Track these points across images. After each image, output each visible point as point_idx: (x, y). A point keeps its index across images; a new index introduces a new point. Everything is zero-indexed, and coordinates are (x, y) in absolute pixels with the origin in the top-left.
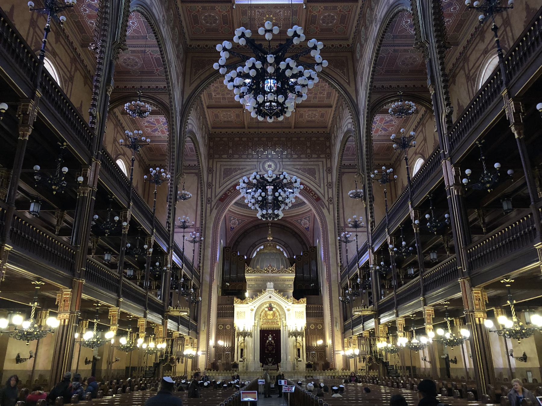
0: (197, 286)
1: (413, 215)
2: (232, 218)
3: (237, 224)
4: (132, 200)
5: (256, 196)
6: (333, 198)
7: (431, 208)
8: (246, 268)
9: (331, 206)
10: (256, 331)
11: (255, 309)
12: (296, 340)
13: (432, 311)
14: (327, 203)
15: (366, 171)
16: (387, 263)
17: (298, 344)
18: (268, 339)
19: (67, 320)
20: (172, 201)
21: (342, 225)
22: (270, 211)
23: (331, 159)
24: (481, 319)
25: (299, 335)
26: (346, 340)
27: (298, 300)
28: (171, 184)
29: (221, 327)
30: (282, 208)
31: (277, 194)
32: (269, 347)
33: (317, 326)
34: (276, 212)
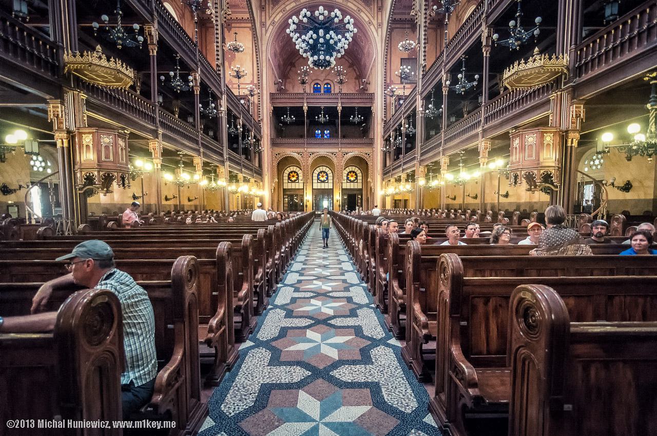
0: (258, 137)
1: (486, 35)
4: (155, 13)
5: (307, 38)
7: (518, 14)
13: (490, 144)
15: (423, 7)
16: (438, 105)
19: (65, 141)
20: (219, 40)
21: (388, 81)
22: (322, 57)
23: (381, 12)
24: (574, 140)
26: (384, 183)
28: (216, 21)
30: (334, 57)
31: (328, 36)
34: (328, 58)
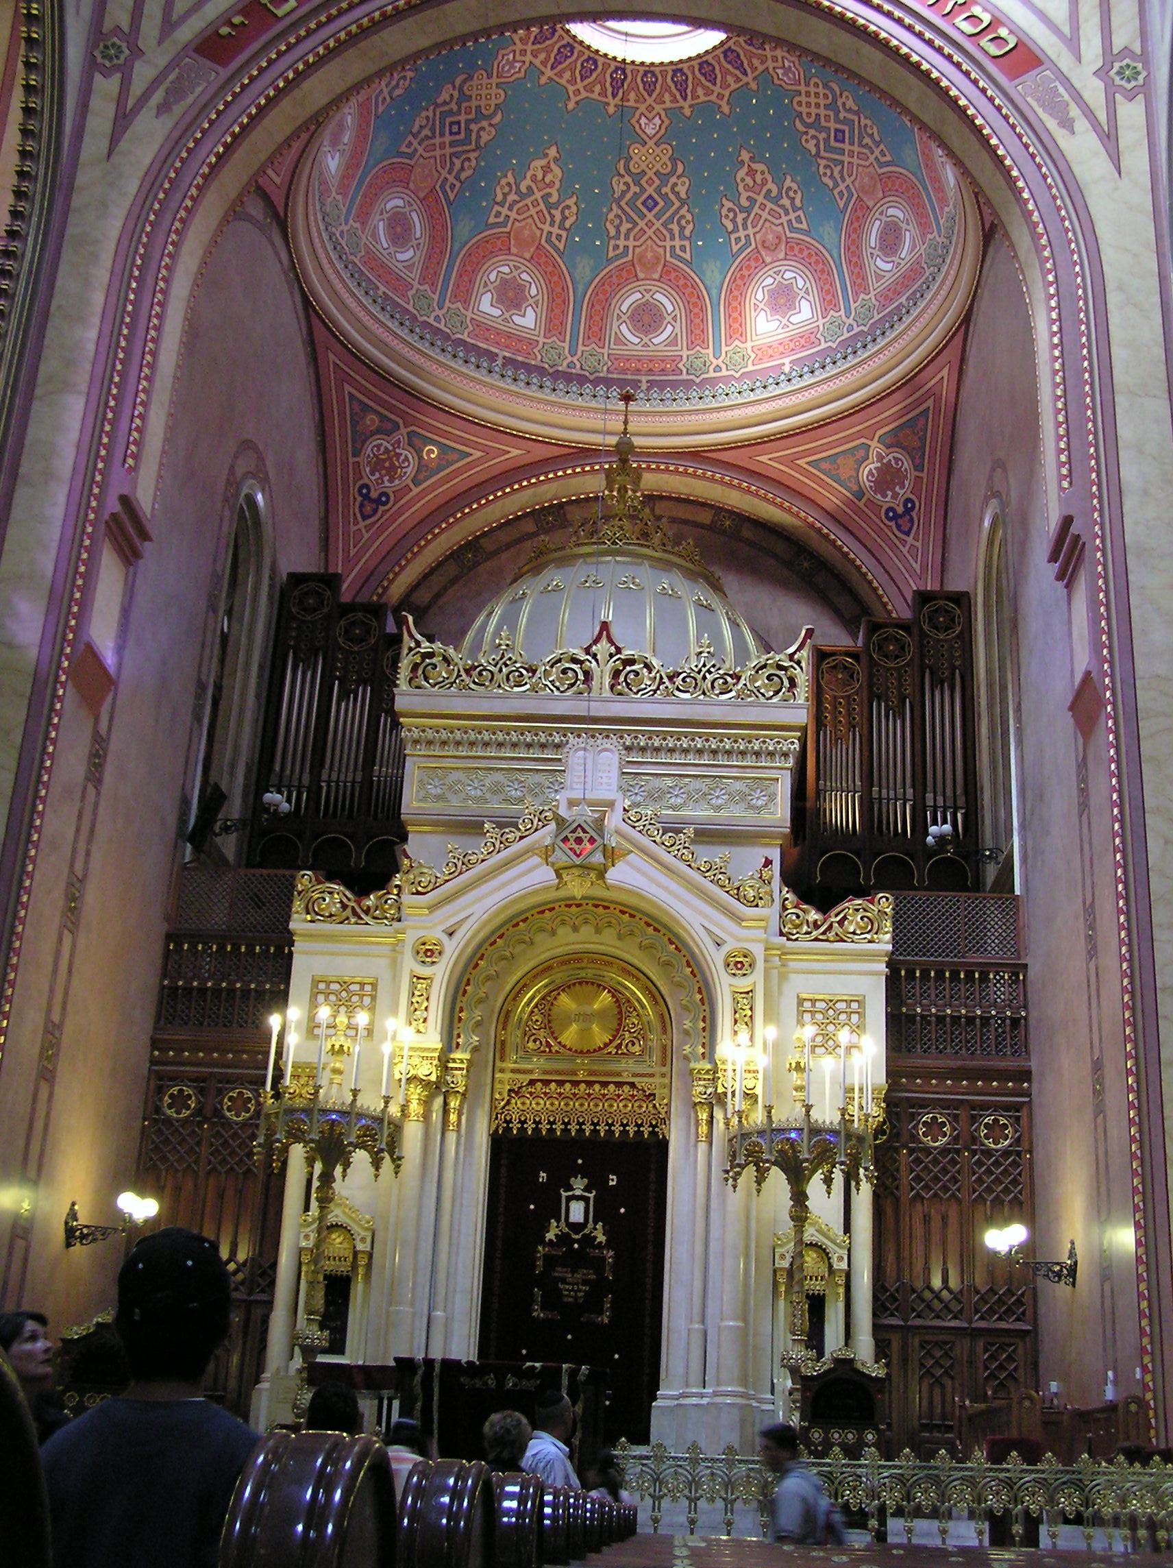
2: (371, 420)
3: (410, 470)
6: (1145, 57)
8: (408, 642)
9: (1131, 114)
10: (452, 1137)
11: (452, 950)
12: (799, 1198)
14: (1094, 92)
17: (810, 1258)
18: (553, 1209)
25: (824, 1155)
27: (824, 908)
29: (179, 1101)
32: (558, 1272)
33: (974, 1119)
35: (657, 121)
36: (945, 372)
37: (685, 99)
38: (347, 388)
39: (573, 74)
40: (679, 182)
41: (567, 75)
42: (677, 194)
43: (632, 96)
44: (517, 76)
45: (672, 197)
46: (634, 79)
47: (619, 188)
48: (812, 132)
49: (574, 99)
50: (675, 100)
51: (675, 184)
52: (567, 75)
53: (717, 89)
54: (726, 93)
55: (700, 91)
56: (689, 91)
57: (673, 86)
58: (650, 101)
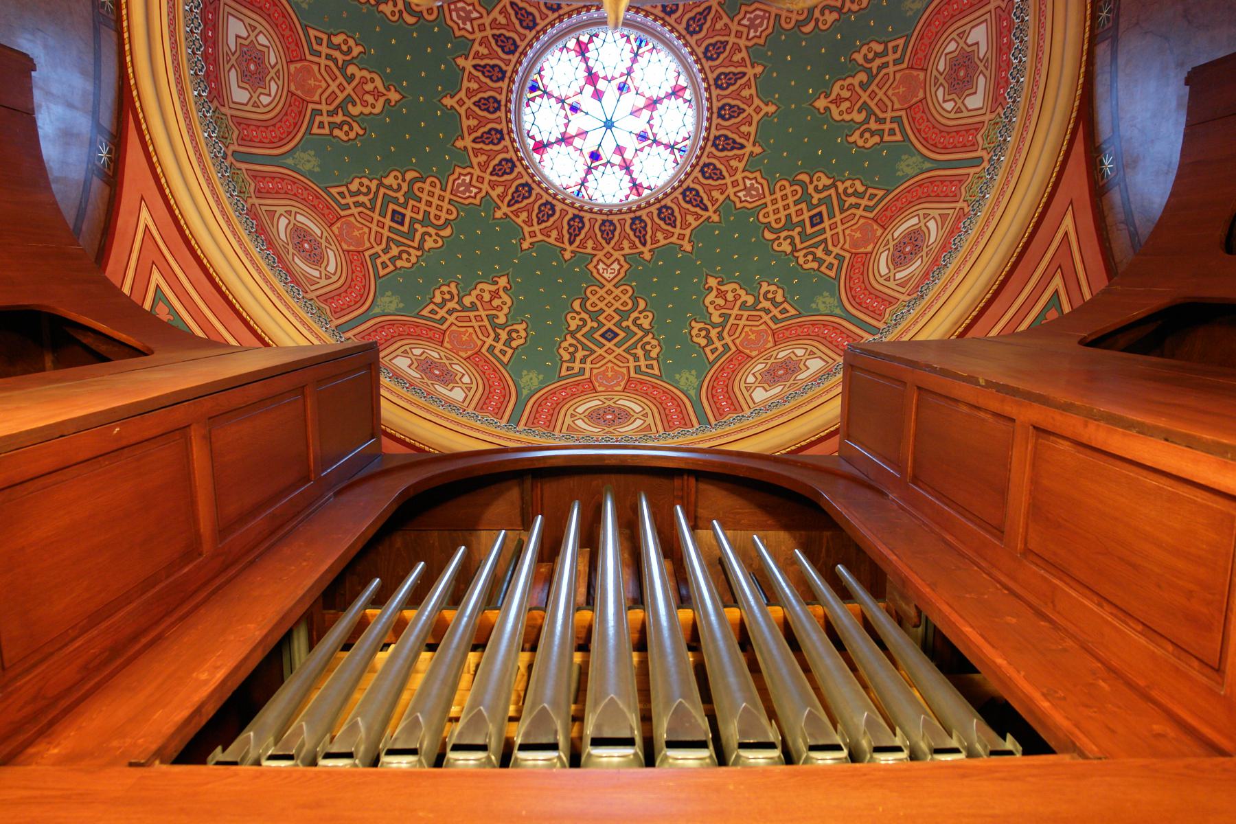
35: (616, 266)
36: (1068, 222)
37: (644, 244)
38: (156, 277)
39: (530, 216)
40: (641, 316)
41: (524, 216)
42: (640, 327)
43: (590, 244)
44: (471, 200)
45: (635, 329)
46: (592, 227)
47: (573, 325)
48: (785, 233)
49: (529, 240)
50: (633, 246)
51: (638, 318)
52: (524, 216)
53: (677, 231)
54: (687, 232)
55: (660, 236)
56: (648, 237)
57: (631, 233)
58: (608, 248)
